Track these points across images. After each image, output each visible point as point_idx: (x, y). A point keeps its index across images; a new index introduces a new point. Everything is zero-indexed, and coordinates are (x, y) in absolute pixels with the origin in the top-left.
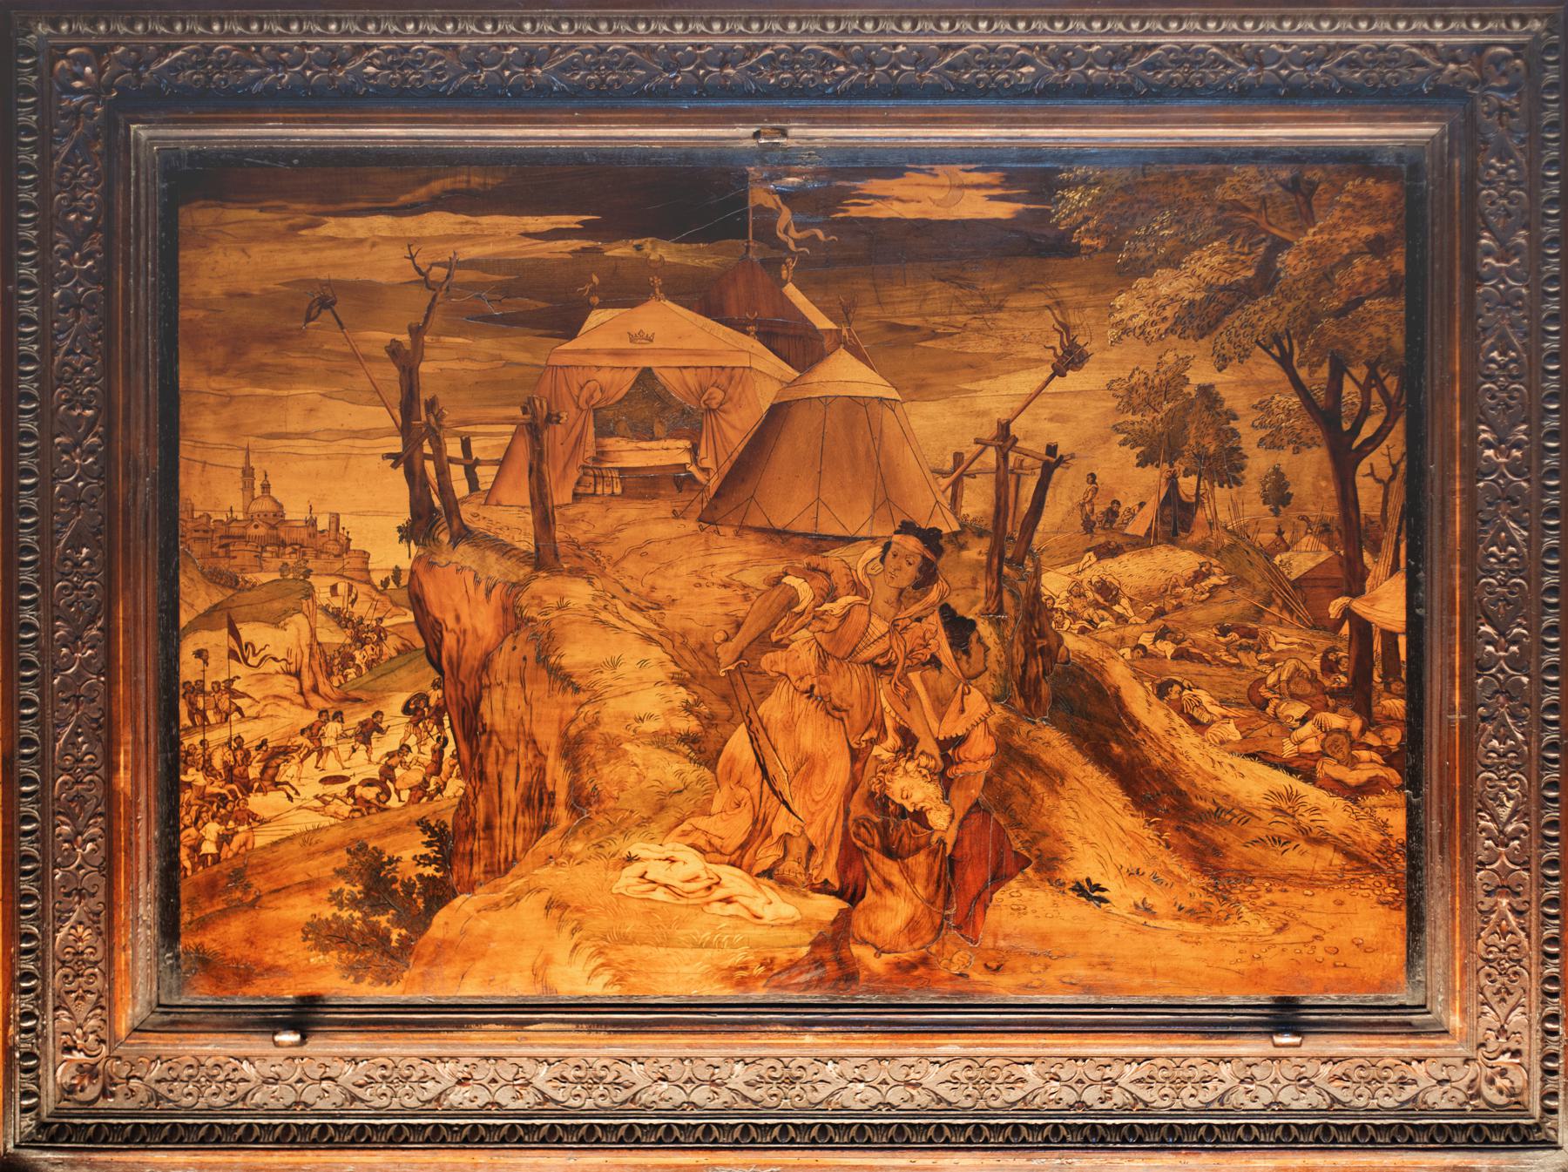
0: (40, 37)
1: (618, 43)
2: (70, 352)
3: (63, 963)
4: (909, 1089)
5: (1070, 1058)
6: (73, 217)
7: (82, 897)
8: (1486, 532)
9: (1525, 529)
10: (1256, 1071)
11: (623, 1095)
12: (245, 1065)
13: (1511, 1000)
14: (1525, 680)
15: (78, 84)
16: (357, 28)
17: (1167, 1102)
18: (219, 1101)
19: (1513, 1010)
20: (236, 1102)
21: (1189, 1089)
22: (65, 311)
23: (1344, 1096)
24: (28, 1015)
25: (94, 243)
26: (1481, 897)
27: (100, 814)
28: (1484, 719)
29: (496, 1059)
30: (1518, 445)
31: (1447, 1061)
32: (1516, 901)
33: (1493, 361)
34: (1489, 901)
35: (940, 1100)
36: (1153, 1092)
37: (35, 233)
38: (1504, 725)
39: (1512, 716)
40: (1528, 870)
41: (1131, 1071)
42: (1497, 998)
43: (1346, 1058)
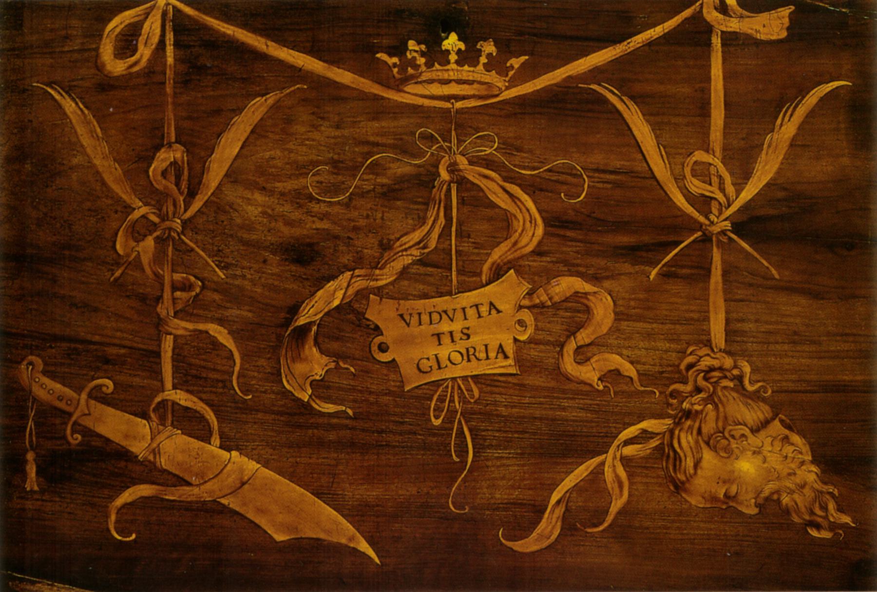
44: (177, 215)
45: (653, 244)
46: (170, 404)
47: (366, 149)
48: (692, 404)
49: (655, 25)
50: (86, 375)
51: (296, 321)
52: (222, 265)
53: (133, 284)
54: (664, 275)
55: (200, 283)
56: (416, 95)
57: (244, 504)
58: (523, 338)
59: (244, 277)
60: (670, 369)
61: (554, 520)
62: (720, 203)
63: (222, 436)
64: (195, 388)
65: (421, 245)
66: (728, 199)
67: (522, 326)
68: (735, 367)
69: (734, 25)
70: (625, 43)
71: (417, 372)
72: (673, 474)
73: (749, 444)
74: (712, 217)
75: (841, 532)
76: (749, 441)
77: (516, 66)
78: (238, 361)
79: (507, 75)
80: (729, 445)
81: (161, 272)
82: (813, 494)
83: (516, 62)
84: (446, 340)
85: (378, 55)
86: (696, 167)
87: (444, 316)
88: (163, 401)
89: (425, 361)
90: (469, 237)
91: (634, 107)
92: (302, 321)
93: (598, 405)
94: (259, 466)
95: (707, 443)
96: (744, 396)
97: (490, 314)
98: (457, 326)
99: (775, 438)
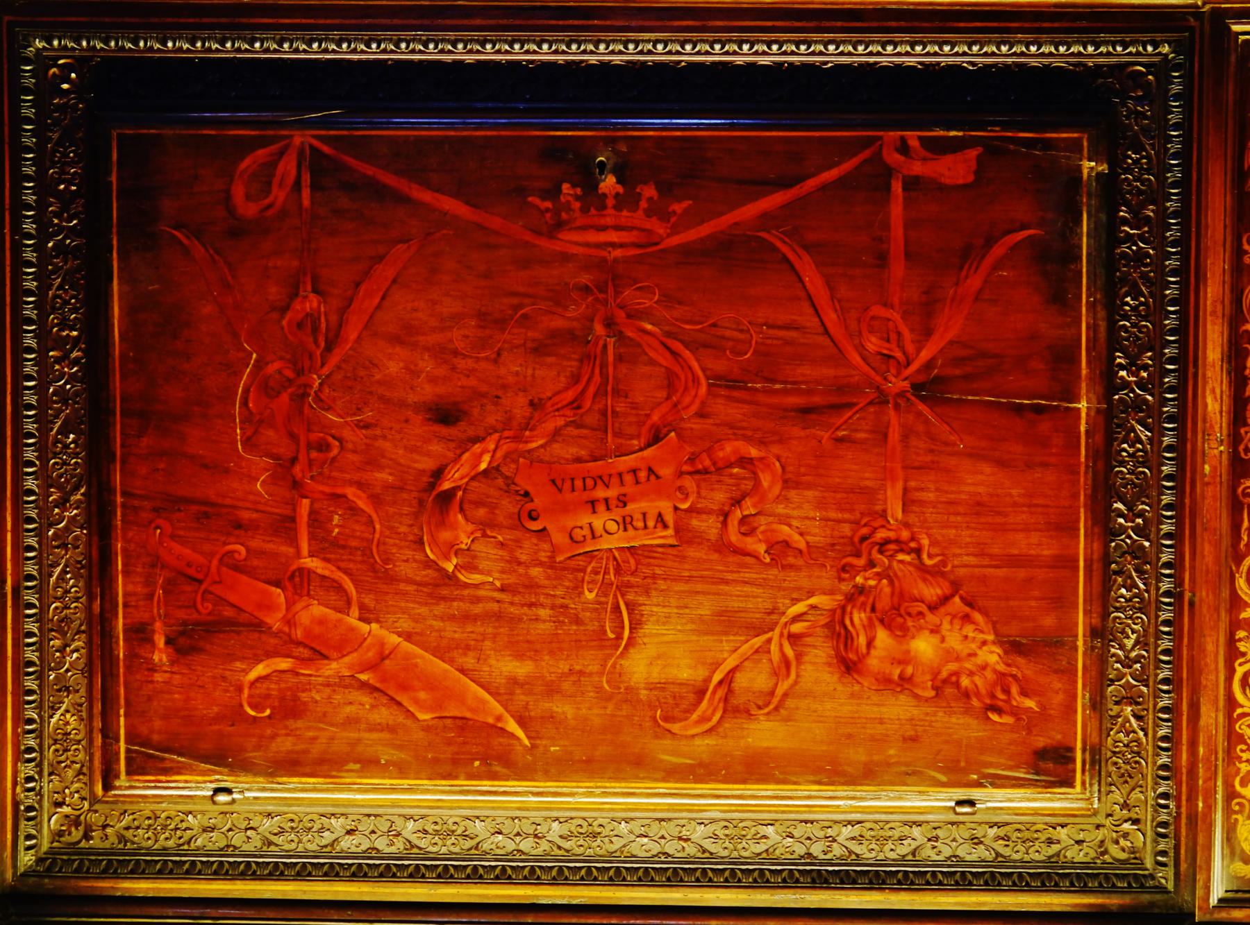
0: (38, 49)
4: (682, 843)
5: (801, 821)
6: (62, 187)
7: (69, 692)
8: (1120, 433)
10: (939, 832)
11: (469, 844)
12: (190, 818)
13: (1132, 782)
14: (1147, 544)
15: (65, 86)
16: (275, 46)
17: (873, 854)
18: (171, 843)
19: (1133, 789)
20: (183, 845)
21: (890, 845)
23: (1006, 852)
24: (29, 779)
26: (1111, 705)
27: (83, 632)
29: (376, 816)
33: (1127, 304)
34: (1116, 708)
35: (704, 851)
36: (863, 847)
37: (34, 198)
38: (1131, 577)
39: (1136, 571)
40: (1146, 686)
41: (847, 831)
42: (1122, 780)
43: (1007, 824)
47: (515, 301)
48: (866, 579)
49: (830, 168)
50: (217, 540)
51: (440, 485)
52: (361, 424)
55: (337, 443)
57: (383, 680)
58: (685, 506)
59: (384, 437)
62: (899, 362)
63: (362, 607)
64: (333, 556)
65: (575, 405)
68: (913, 539)
69: (917, 168)
71: (567, 540)
73: (926, 622)
75: (1024, 717)
76: (927, 619)
77: (679, 211)
78: (378, 526)
79: (669, 221)
81: (296, 430)
82: (995, 676)
83: (678, 207)
84: (601, 508)
85: (530, 199)
87: (599, 483)
90: (626, 397)
91: (807, 258)
92: (446, 486)
93: (763, 579)
94: (400, 639)
95: (882, 621)
97: (648, 480)
98: (612, 493)
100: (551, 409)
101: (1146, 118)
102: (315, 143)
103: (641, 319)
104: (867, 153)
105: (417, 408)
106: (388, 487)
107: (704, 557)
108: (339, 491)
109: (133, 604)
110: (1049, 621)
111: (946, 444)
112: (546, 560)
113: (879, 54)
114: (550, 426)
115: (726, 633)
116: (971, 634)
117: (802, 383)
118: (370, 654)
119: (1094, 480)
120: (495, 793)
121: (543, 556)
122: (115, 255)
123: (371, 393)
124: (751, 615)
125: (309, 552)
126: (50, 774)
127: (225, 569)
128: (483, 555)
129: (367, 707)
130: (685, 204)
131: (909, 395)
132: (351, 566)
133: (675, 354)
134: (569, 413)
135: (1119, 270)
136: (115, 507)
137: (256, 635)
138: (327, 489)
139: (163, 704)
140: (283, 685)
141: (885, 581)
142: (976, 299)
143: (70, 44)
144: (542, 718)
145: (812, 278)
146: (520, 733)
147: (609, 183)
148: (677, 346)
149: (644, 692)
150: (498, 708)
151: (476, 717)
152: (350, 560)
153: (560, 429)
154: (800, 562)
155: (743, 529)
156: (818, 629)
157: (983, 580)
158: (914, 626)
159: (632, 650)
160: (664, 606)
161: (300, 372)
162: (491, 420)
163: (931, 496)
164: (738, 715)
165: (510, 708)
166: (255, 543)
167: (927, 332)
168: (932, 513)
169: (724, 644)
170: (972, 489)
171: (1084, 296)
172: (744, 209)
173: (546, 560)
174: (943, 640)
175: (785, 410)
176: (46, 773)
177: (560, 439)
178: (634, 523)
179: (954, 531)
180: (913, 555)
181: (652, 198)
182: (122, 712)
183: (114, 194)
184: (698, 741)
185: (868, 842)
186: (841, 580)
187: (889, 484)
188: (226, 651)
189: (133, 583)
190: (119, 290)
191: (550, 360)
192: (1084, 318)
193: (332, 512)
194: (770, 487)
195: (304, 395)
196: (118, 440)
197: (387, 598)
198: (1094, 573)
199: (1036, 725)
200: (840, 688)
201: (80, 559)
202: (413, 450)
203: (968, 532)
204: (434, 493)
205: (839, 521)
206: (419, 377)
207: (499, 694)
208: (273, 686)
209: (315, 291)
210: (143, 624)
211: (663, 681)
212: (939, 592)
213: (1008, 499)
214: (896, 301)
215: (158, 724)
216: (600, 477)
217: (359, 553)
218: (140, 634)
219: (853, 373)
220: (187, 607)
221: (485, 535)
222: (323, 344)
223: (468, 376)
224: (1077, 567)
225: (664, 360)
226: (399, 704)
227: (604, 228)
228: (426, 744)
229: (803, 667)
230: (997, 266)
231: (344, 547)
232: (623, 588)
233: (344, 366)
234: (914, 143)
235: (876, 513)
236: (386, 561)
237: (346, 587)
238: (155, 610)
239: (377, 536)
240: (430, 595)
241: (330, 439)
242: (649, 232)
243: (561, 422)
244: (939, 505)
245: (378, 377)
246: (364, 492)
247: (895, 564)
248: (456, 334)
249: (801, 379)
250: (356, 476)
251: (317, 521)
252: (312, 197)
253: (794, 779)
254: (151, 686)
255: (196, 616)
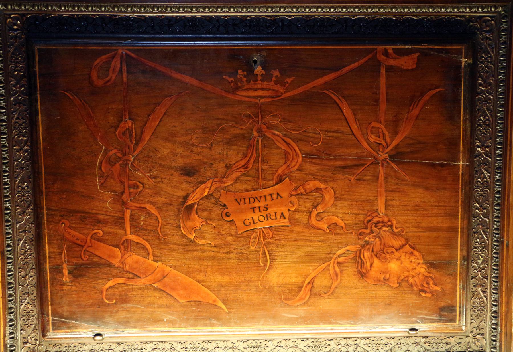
1: (199, 15)
2: (17, 118)
3: (23, 315)
6: (16, 73)
9: (489, 173)
13: (481, 319)
14: (488, 220)
15: (15, 27)
19: (481, 321)
22: (15, 105)
24: (11, 333)
25: (24, 82)
27: (34, 268)
28: (474, 233)
30: (488, 147)
31: (461, 337)
32: (483, 288)
33: (481, 120)
34: (474, 289)
37: (3, 78)
38: (481, 234)
39: (483, 232)
40: (487, 279)
43: (429, 337)
44: (130, 154)
45: (351, 166)
46: (129, 241)
47: (219, 122)
48: (370, 238)
49: (354, 62)
50: (90, 228)
53: (110, 186)
54: (357, 180)
55: (142, 185)
56: (242, 96)
57: (165, 286)
60: (359, 222)
61: (307, 291)
62: (383, 146)
63: (154, 256)
64: (141, 234)
65: (245, 167)
66: (387, 145)
67: (292, 204)
68: (389, 221)
69: (392, 62)
70: (341, 71)
71: (244, 225)
72: (360, 270)
74: (380, 153)
76: (395, 254)
77: (289, 82)
78: (160, 221)
79: (285, 86)
80: (386, 256)
81: (123, 180)
82: (423, 278)
83: (289, 80)
84: (257, 210)
85: (224, 77)
86: (372, 129)
88: (126, 240)
89: (248, 220)
90: (267, 163)
92: (190, 202)
93: (327, 239)
94: (171, 269)
95: (376, 256)
96: (393, 234)
97: (277, 198)
98: (262, 204)
99: (406, 253)
100: (235, 169)
101: (490, 40)
102: (128, 52)
103: (273, 129)
104: (370, 56)
105: (176, 169)
106: (164, 204)
107: (301, 231)
108: (143, 206)
109: (53, 257)
110: (446, 254)
111: (403, 181)
112: (234, 233)
113: (377, 12)
114: (234, 176)
115: (310, 263)
116: (413, 260)
117: (342, 156)
118: (158, 275)
119: (465, 194)
120: (213, 332)
121: (232, 232)
122: (39, 103)
123: (156, 163)
124: (321, 255)
125: (131, 232)
126: (21, 330)
127: (93, 240)
128: (206, 232)
129: (158, 298)
130: (292, 78)
131: (388, 160)
132: (149, 238)
133: (288, 144)
134: (242, 170)
135: (477, 105)
136: (44, 215)
137: (108, 268)
138: (138, 205)
139: (68, 299)
140: (121, 290)
141: (377, 239)
142: (416, 119)
143: (17, 8)
144: (233, 300)
145: (347, 111)
146: (224, 307)
147: (258, 70)
148: (289, 141)
149: (276, 288)
150: (215, 297)
151: (204, 301)
152: (148, 235)
153: (239, 177)
154: (342, 232)
155: (318, 218)
156: (349, 260)
157: (418, 237)
158: (390, 258)
159: (271, 271)
160: (285, 252)
161: (124, 155)
162: (209, 174)
163: (397, 203)
164: (316, 296)
165: (219, 296)
166: (107, 229)
167: (395, 133)
168: (397, 210)
169: (310, 267)
170: (414, 199)
171: (462, 117)
172: (317, 80)
173: (234, 233)
174: (402, 263)
175: (336, 167)
176: (19, 330)
177: (239, 182)
178: (271, 217)
179: (406, 217)
180: (389, 228)
181: (277, 76)
182: (50, 303)
183: (38, 76)
184: (299, 308)
185: (372, 346)
186: (359, 239)
187: (379, 198)
188: (95, 276)
189: (53, 248)
190: (42, 119)
191: (234, 147)
192: (462, 126)
193: (140, 215)
194: (329, 200)
195: (127, 164)
196: (44, 185)
197: (165, 251)
198: (464, 234)
199: (440, 297)
200: (359, 284)
201: (32, 237)
202: (176, 187)
203: (413, 218)
204: (184, 206)
205: (358, 214)
206: (177, 156)
207: (214, 291)
208: (116, 290)
209: (130, 118)
210: (58, 265)
211: (284, 283)
212: (400, 243)
213: (429, 204)
214: (383, 120)
215: (66, 308)
216: (257, 198)
217: (152, 232)
218: (57, 270)
219: (364, 151)
220: (77, 257)
221: (207, 223)
222: (134, 142)
223: (198, 155)
224: (458, 231)
225: (283, 146)
226: (172, 296)
227: (257, 90)
228: (183, 312)
229: (343, 276)
230: (424, 105)
231: (146, 230)
232: (267, 245)
233: (143, 151)
234: (390, 51)
235: (374, 210)
236: (164, 235)
237: (147, 247)
238: (63, 259)
239: (160, 225)
240: (184, 250)
241: (138, 183)
242: (276, 91)
243: (239, 174)
244: (401, 207)
245: (159, 156)
246: (154, 206)
247: (382, 232)
248: (193, 137)
249: (342, 154)
250: (150, 199)
251: (133, 218)
252: (127, 77)
253: (340, 322)
254: (62, 292)
255: (81, 261)
